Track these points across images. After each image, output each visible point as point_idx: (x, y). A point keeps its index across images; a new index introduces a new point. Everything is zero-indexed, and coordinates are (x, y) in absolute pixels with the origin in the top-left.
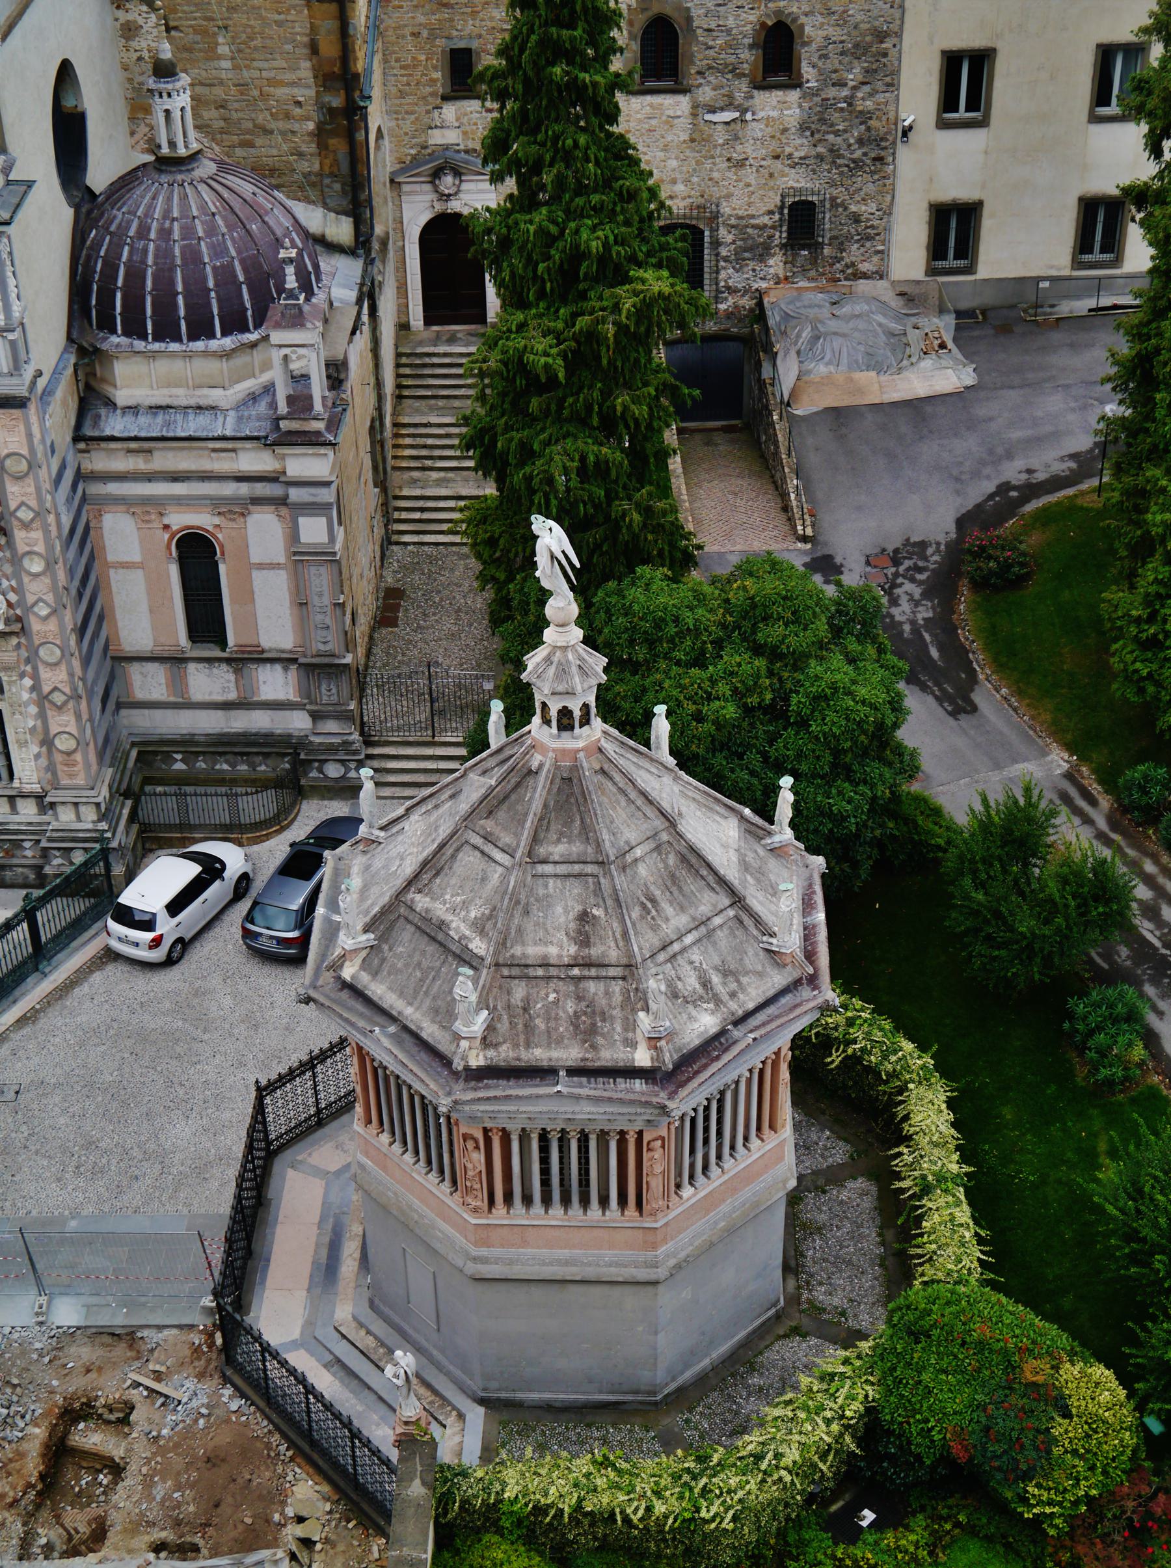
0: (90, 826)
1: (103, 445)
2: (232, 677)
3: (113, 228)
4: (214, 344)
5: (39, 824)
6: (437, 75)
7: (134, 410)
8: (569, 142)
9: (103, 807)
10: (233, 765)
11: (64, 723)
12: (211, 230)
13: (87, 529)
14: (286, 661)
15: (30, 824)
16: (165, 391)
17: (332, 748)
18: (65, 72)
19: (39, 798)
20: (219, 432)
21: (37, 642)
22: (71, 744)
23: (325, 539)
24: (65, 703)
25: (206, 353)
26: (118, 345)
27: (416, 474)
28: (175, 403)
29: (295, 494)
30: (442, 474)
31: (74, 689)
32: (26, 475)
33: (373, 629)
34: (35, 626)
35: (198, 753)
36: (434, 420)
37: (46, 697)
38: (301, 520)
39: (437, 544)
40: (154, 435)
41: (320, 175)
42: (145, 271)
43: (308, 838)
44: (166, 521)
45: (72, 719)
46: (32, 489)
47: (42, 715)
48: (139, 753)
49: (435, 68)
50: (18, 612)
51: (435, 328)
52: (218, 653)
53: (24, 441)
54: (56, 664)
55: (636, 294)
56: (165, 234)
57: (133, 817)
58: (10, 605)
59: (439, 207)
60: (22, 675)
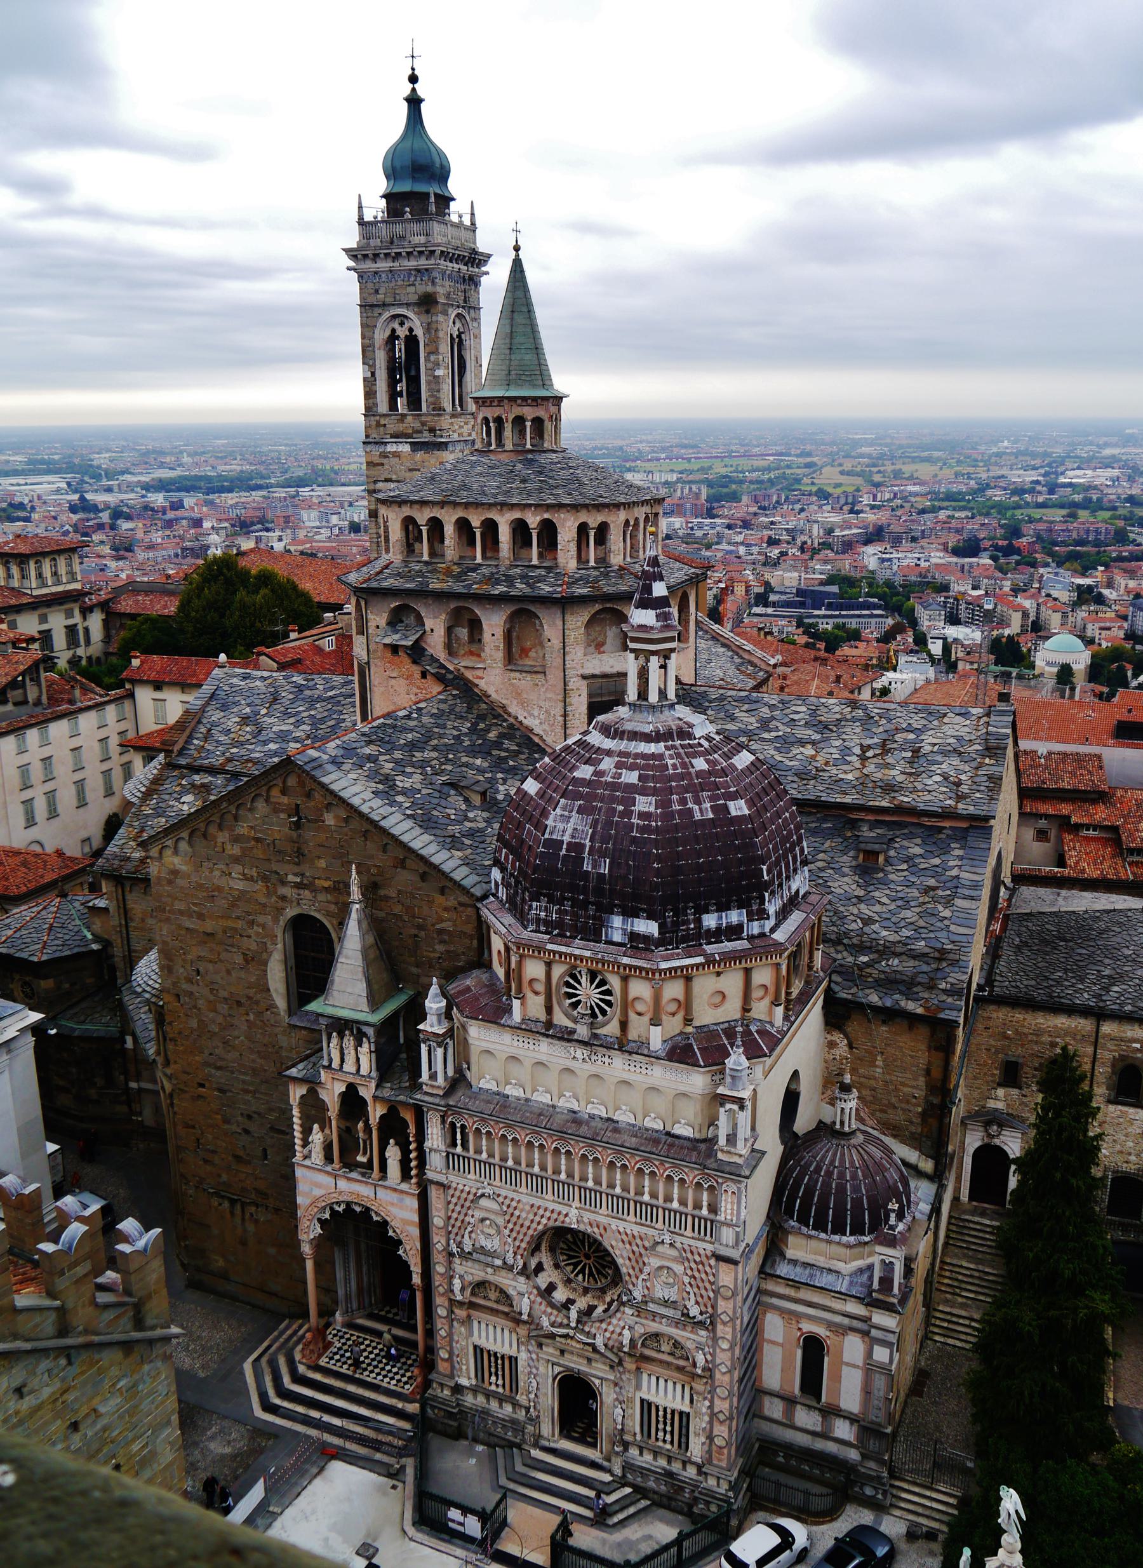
2: (820, 1419)
4: (845, 1239)
6: (997, 1072)
7: (794, 1262)
8: (1060, 1211)
11: (721, 1431)
12: (854, 1177)
13: (757, 1318)
14: (852, 1419)
16: (813, 1256)
17: (870, 1478)
18: (795, 1075)
19: (699, 1468)
20: (838, 1289)
22: (723, 1443)
23: (887, 1360)
24: (725, 1421)
25: (839, 1243)
27: (948, 1296)
28: (818, 1264)
29: (874, 1332)
30: (964, 1300)
31: (731, 1413)
33: (908, 1396)
34: (718, 1376)
36: (965, 1264)
38: (875, 1347)
39: (955, 1346)
41: (921, 1135)
43: (846, 1536)
46: (731, 1306)
47: (711, 1423)
49: (996, 1068)
51: (974, 1203)
52: (814, 1404)
55: (1087, 1307)
56: (829, 1174)
57: (748, 1489)
58: (706, 1361)
59: (986, 1140)
60: (705, 1399)
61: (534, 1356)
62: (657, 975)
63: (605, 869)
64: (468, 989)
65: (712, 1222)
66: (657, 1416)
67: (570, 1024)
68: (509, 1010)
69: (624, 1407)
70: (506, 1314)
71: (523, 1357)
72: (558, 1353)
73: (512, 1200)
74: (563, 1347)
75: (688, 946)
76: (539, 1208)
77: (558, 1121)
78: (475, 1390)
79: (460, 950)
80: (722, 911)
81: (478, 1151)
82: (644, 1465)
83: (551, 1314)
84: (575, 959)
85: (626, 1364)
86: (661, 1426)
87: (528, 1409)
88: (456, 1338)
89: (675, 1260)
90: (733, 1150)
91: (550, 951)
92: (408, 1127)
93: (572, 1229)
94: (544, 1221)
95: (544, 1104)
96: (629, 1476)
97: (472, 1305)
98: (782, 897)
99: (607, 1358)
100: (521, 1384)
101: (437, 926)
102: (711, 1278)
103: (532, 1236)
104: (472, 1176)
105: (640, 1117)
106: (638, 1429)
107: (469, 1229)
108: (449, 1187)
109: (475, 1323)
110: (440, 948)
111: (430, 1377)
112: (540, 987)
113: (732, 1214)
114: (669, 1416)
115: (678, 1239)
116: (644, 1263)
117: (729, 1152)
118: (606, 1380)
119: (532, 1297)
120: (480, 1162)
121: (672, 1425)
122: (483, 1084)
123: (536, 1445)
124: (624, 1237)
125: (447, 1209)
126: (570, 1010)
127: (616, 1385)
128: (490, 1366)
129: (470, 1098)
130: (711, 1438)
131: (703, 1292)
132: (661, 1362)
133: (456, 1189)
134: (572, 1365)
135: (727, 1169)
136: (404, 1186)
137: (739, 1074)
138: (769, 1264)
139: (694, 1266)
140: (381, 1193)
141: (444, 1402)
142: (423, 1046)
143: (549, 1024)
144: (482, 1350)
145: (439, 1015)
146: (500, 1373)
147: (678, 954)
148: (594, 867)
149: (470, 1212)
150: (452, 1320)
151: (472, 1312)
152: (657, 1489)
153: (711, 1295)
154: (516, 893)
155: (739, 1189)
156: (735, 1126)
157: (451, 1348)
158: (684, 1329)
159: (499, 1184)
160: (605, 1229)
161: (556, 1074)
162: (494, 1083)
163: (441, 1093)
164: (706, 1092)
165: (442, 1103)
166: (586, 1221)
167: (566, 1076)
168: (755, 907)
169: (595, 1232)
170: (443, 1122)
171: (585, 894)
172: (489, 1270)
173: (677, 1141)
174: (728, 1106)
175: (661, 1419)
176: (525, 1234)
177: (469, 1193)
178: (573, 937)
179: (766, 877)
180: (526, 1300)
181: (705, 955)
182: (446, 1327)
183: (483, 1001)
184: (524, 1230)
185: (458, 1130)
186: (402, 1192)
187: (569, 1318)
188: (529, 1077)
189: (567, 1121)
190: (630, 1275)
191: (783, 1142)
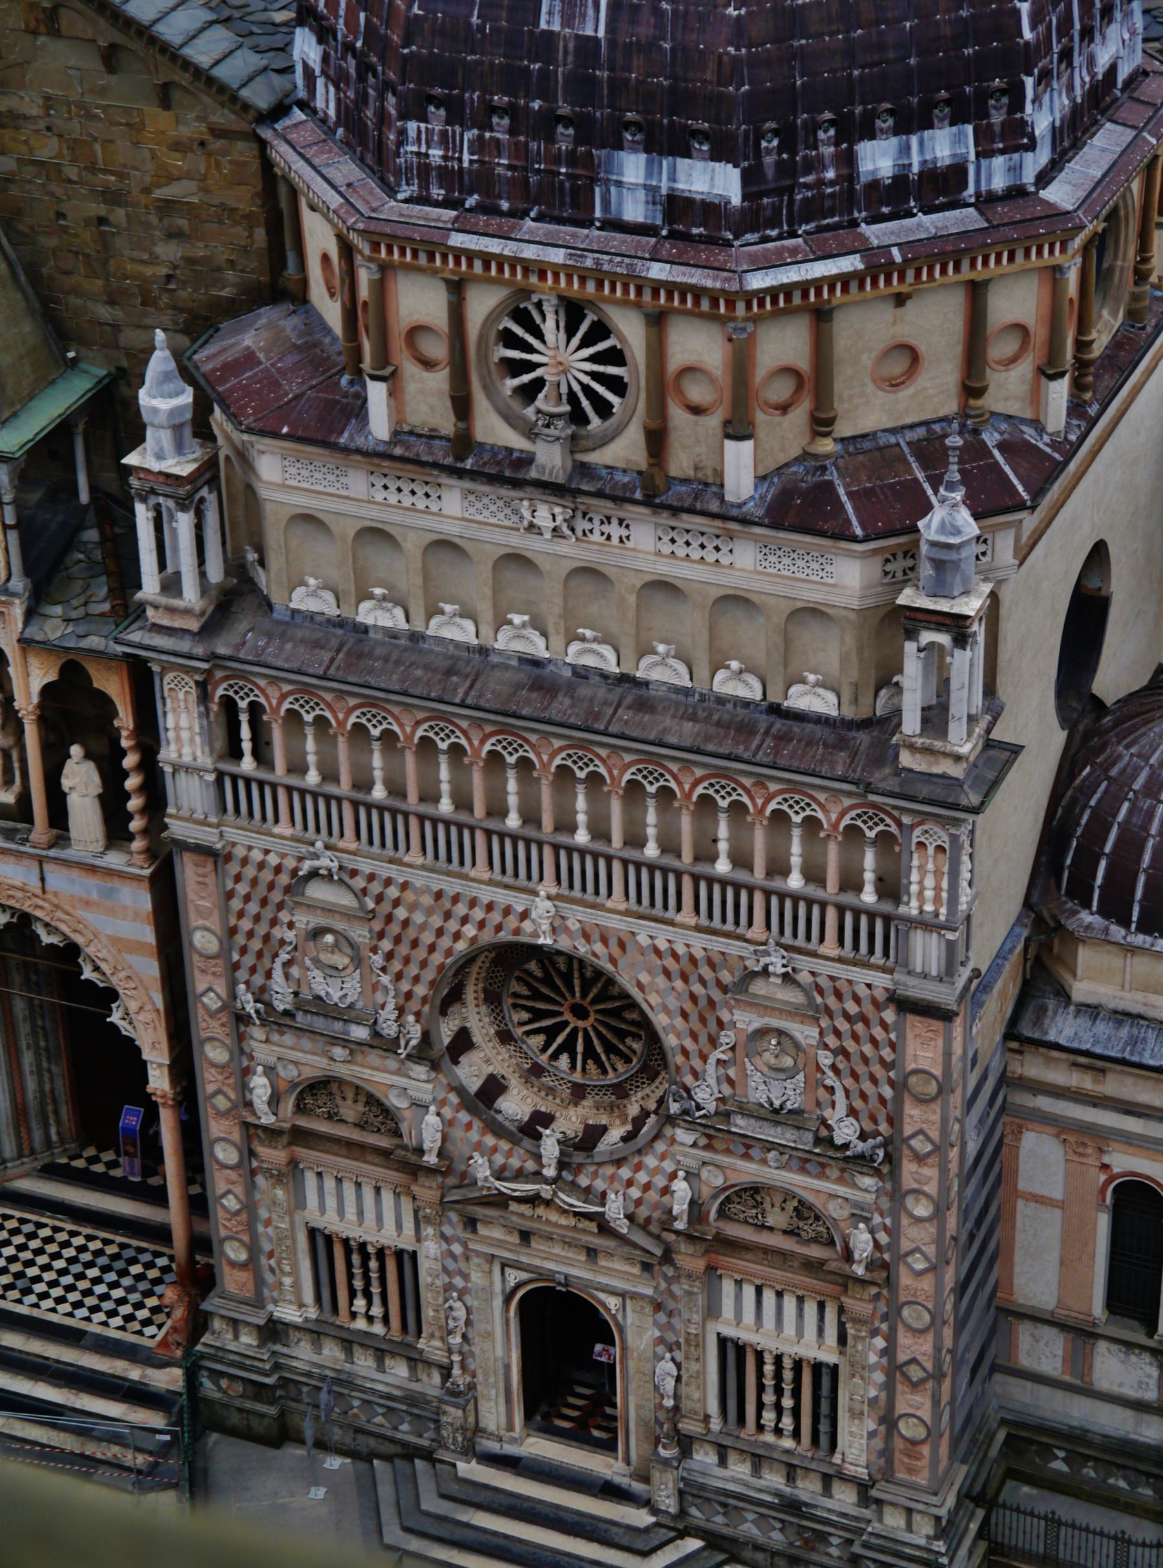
0: (922, 1542)
1: (1042, 1050)
3: (1114, 772)
5: (857, 1519)
7: (1092, 1011)
9: (944, 1523)
10: (1133, 1485)
13: (1000, 1144)
15: (844, 1515)
16: (1140, 996)
18: (1099, 554)
19: (863, 1488)
21: (902, 1298)
22: (921, 1433)
24: (923, 1381)
26: (1089, 927)
28: (1151, 1013)
31: (938, 1363)
32: (933, 1099)
34: (905, 1279)
35: (1088, 1458)
37: (900, 1367)
40: (1113, 1054)
42: (1145, 840)
44: (1106, 1159)
45: (928, 1404)
46: (936, 1118)
47: (889, 1387)
48: (1009, 1435)
50: (886, 1256)
53: (940, 1060)
54: (922, 1332)
57: (981, 1534)
58: (877, 1245)
60: (874, 1333)
61: (457, 1249)
62: (740, 308)
63: (596, 26)
64: (249, 359)
65: (887, 919)
66: (760, 1374)
67: (515, 441)
68: (358, 409)
69: (679, 1356)
70: (385, 1154)
71: (430, 1250)
72: (515, 1239)
73: (388, 882)
74: (528, 1225)
75: (820, 230)
76: (456, 899)
77: (494, 688)
78: (315, 1333)
79: (222, 255)
80: (909, 131)
81: (297, 767)
82: (731, 1487)
83: (495, 1150)
84: (526, 271)
85: (680, 1260)
86: (769, 1398)
87: (446, 1372)
88: (263, 1213)
89: (794, 1013)
90: (938, 744)
91: (458, 253)
92: (115, 714)
93: (539, 948)
94: (470, 931)
95: (457, 645)
96: (694, 1511)
97: (299, 1136)
98: (1070, 88)
99: (635, 1246)
100: (428, 1313)
101: (158, 193)
102: (887, 1053)
103: (441, 967)
104: (283, 829)
105: (702, 671)
106: (713, 1407)
107: (284, 957)
108: (228, 857)
109: (310, 1179)
110: (170, 251)
111: (205, 1306)
112: (437, 349)
113: (937, 900)
114: (788, 1375)
115: (804, 963)
116: (721, 1024)
117: (927, 751)
118: (634, 1296)
119: (447, 1112)
120: (303, 792)
121: (796, 1394)
122: (301, 600)
123: (469, 1451)
124: (670, 963)
125: (226, 910)
126: (516, 405)
127: (658, 1307)
128: (350, 1276)
129: (270, 636)
130: (889, 1421)
131: (867, 1086)
132: (768, 1252)
133: (245, 861)
134: (551, 1266)
135: (924, 791)
136: (115, 860)
137: (954, 556)
138: (1028, 1016)
139: (843, 1025)
140: (57, 878)
141: (242, 1361)
142: (140, 509)
143: (464, 443)
144: (329, 1239)
145: (177, 429)
146: (375, 1290)
147: (794, 251)
148: (567, 21)
149: (284, 916)
150: (253, 1173)
151: (301, 1152)
152: (761, 1540)
153: (887, 1092)
154: (363, 98)
155: (954, 839)
156: (944, 687)
157: (254, 1236)
158: (822, 1176)
159: (353, 846)
160: (622, 945)
161: (486, 570)
162: (329, 596)
163: (194, 625)
164: (870, 602)
165: (199, 650)
166: (573, 925)
167: (510, 574)
168: (997, 118)
169: (596, 953)
170: (204, 696)
171: (546, 93)
172: (339, 1052)
173: (796, 728)
174: (927, 637)
175: (769, 1382)
176: (424, 964)
177: (278, 869)
178: (519, 214)
179: (1028, 35)
180: (431, 1119)
181: (865, 250)
182: (239, 1190)
183: (291, 388)
184: (421, 953)
185: (244, 718)
186: (110, 873)
187: (538, 1157)
188: (418, 581)
189: (519, 686)
190: (685, 1052)
191: (1065, 721)
